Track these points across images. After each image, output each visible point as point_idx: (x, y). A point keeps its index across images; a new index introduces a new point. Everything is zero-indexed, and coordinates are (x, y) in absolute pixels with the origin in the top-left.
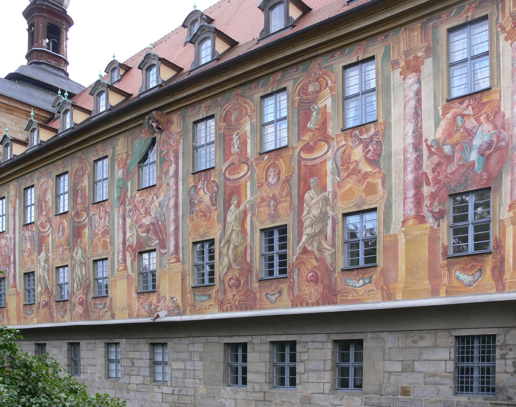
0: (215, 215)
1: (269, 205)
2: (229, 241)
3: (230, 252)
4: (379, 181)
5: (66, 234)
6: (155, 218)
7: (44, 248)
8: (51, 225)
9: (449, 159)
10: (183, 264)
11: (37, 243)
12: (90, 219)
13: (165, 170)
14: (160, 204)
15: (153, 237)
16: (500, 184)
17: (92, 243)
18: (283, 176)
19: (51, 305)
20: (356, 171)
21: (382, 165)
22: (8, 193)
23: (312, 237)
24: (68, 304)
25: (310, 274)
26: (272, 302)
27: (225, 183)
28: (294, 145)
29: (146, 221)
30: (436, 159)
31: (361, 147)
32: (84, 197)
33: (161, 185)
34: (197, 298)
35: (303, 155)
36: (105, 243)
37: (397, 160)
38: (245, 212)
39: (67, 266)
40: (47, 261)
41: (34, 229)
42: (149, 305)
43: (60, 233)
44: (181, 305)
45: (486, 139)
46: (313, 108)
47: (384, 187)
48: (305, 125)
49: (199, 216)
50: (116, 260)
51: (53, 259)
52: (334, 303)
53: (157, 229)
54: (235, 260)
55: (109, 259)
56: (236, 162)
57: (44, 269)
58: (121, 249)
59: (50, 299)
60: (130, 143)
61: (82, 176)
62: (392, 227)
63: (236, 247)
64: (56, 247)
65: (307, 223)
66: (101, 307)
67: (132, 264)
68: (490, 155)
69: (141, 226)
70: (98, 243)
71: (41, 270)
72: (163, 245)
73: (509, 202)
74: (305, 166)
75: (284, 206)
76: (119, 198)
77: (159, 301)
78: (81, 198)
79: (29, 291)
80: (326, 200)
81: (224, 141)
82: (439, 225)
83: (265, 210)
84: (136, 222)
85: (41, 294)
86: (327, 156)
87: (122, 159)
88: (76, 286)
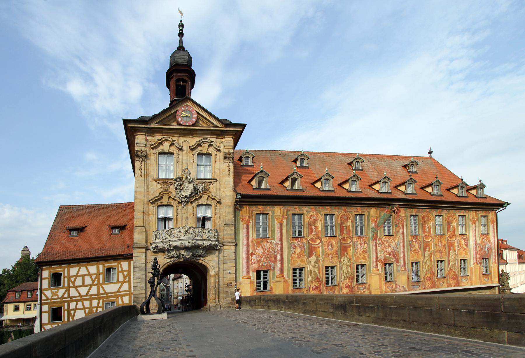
0: (420, 253)
2: (426, 263)
5: (334, 248)
8: (321, 241)
14: (396, 244)
15: (393, 257)
19: (321, 287)
29: (389, 250)
32: (348, 231)
38: (431, 254)
40: (317, 262)
41: (305, 241)
43: (330, 247)
51: (323, 261)
52: (459, 286)
54: (428, 270)
57: (314, 266)
59: (320, 285)
63: (428, 266)
64: (325, 255)
65: (451, 261)
67: (381, 268)
69: (386, 252)
72: (398, 261)
75: (444, 254)
76: (373, 237)
80: (456, 254)
83: (438, 255)
84: (383, 250)
85: (311, 282)
88: (343, 277)
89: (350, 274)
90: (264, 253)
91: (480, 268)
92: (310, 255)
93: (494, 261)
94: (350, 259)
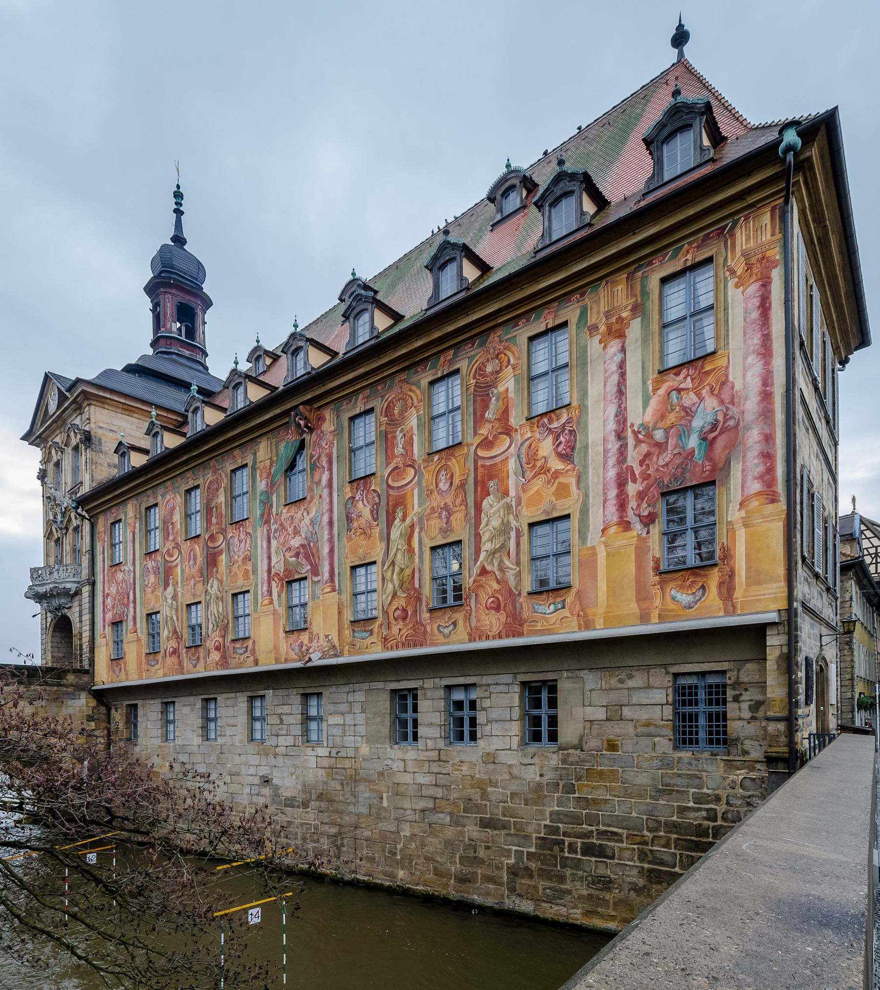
0: (376, 531)
1: (440, 517)
2: (393, 563)
3: (395, 576)
4: (573, 481)
5: (198, 563)
6: (306, 538)
7: (171, 581)
8: (180, 552)
9: (661, 447)
10: (340, 593)
11: (162, 575)
12: (228, 544)
13: (316, 479)
15: (304, 561)
16: (728, 475)
17: (230, 572)
18: (456, 481)
20: (544, 470)
21: (576, 460)
22: (126, 514)
23: (494, 552)
24: (201, 650)
25: (491, 600)
26: (446, 637)
27: (388, 492)
28: (470, 441)
29: (296, 542)
30: (644, 448)
31: (550, 439)
33: (312, 498)
34: (356, 635)
35: (481, 453)
36: (247, 571)
37: (595, 453)
38: (412, 527)
39: (200, 602)
40: (175, 597)
41: (159, 558)
42: (299, 646)
43: (191, 562)
44: (337, 644)
45: (710, 419)
46: (492, 393)
47: (579, 488)
48: (483, 416)
49: (358, 534)
50: (260, 592)
51: (183, 595)
53: (308, 552)
54: (401, 587)
55: (252, 592)
56: (401, 465)
57: (171, 608)
58: (266, 578)
60: (274, 447)
61: (217, 490)
62: (589, 537)
63: (402, 570)
64: (185, 580)
65: (485, 537)
66: (242, 651)
67: (279, 596)
68: (715, 438)
70: (238, 572)
71: (168, 609)
72: (315, 571)
73: (739, 498)
74: (483, 466)
75: (458, 518)
76: (262, 515)
77: (311, 640)
78: (217, 518)
79: (153, 636)
80: (509, 507)
81: (386, 439)
82: (648, 533)
83: (436, 524)
84: (283, 544)
85: (168, 639)
86: (508, 453)
87: (265, 467)
88: (211, 626)
89: (221, 617)
90: (118, 592)
91: (642, 542)
92: (166, 585)
93: (756, 487)
94: (221, 582)
